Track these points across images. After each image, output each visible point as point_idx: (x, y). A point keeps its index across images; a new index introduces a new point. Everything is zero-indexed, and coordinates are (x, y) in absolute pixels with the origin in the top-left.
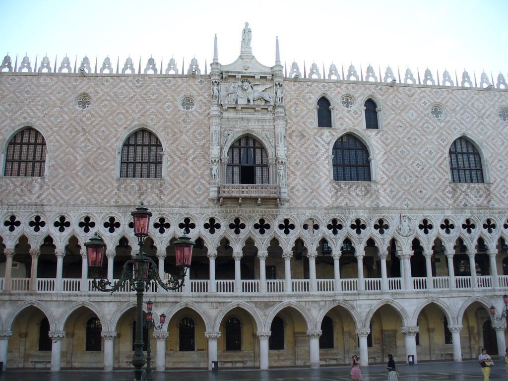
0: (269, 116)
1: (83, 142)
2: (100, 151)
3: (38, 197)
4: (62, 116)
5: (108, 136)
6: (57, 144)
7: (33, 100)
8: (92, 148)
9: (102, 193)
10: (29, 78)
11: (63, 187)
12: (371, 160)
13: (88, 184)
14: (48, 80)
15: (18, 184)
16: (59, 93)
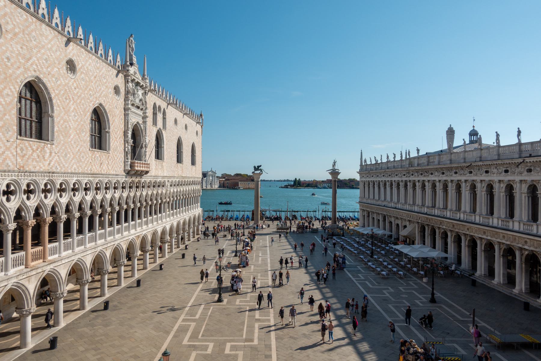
0: (141, 113)
1: (73, 111)
2: (82, 123)
3: (49, 164)
4: (59, 79)
5: (85, 109)
6: (58, 109)
7: (39, 51)
8: (78, 119)
9: (84, 162)
10: (34, 19)
11: (63, 155)
12: (161, 147)
13: (77, 153)
14: (48, 32)
15: (35, 148)
16: (56, 51)
